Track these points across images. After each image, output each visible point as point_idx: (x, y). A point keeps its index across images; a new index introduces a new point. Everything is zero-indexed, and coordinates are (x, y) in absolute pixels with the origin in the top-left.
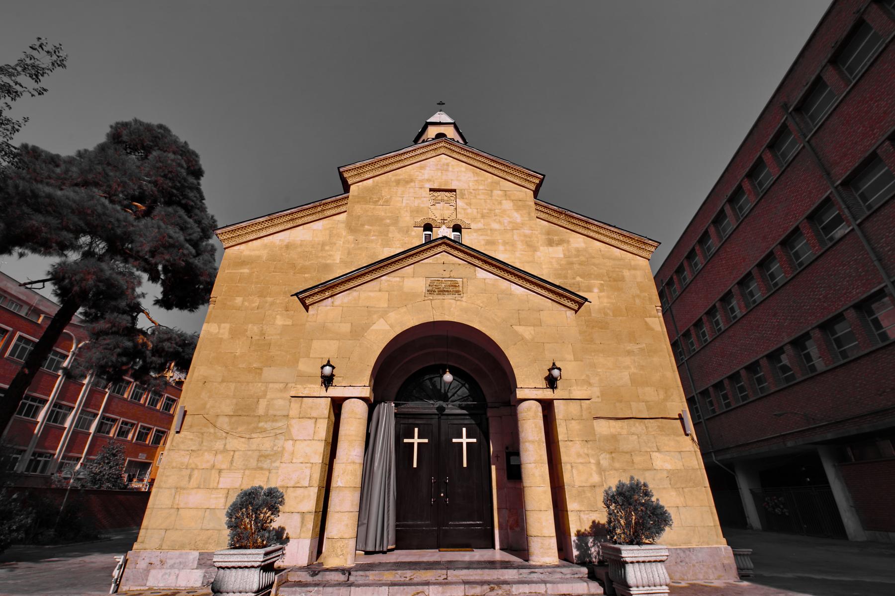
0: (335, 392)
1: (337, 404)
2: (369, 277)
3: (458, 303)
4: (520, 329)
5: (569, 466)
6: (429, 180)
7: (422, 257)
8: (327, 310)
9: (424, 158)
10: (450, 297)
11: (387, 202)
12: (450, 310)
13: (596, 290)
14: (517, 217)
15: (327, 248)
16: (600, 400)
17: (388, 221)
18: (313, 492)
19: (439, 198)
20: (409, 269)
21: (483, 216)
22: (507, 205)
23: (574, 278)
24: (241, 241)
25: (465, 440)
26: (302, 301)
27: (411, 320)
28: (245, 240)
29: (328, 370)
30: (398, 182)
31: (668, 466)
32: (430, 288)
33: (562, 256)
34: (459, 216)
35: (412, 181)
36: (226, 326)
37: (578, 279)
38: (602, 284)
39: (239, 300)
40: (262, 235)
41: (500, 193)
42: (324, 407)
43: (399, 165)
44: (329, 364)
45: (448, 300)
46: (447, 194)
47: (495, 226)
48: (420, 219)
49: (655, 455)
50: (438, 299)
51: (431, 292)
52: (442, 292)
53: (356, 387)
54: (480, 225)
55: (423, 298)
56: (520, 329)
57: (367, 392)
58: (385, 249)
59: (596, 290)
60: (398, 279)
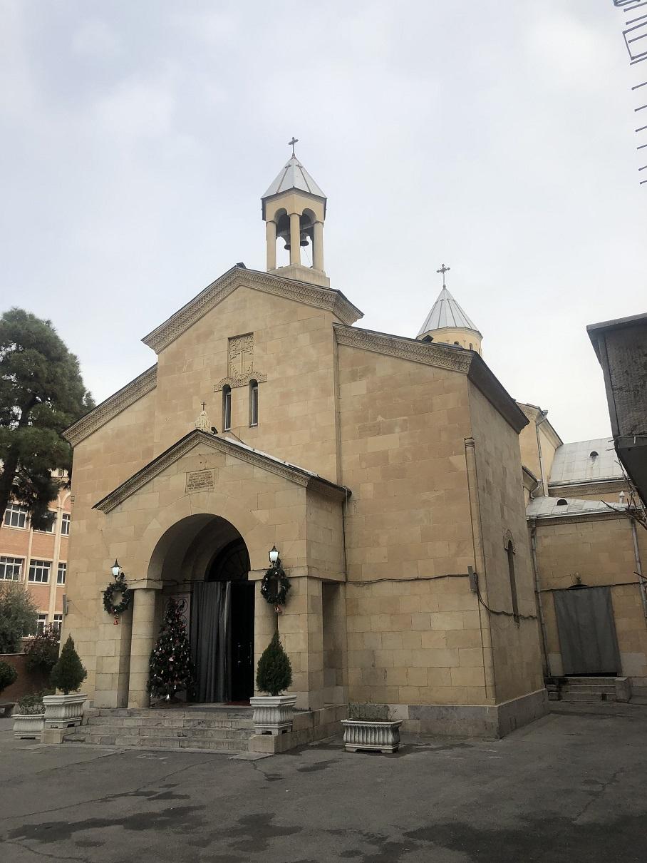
2: (145, 481)
7: (182, 453)
11: (190, 366)
12: (206, 504)
13: (397, 430)
15: (148, 430)
16: (386, 560)
20: (174, 467)
21: (279, 363)
22: (305, 339)
23: (375, 419)
24: (83, 437)
27: (177, 518)
28: (86, 435)
31: (448, 628)
33: (365, 392)
34: (255, 368)
35: (211, 333)
36: (84, 522)
37: (380, 418)
38: (405, 420)
41: (296, 324)
43: (198, 316)
46: (245, 339)
47: (291, 372)
48: (219, 381)
49: (434, 616)
52: (199, 485)
55: (184, 494)
59: (397, 430)
60: (166, 478)
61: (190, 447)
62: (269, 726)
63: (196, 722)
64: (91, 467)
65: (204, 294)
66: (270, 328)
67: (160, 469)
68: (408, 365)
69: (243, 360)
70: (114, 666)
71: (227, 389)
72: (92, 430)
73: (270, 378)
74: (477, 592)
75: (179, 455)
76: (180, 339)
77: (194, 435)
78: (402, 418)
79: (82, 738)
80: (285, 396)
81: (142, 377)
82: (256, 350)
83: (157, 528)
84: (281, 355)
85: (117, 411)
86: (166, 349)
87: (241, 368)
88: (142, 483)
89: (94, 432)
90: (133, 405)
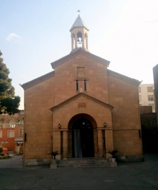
0: (61, 130)
1: (62, 132)
4: (98, 114)
12: (83, 111)
26: (51, 110)
27: (76, 114)
29: (59, 126)
42: (60, 132)
50: (80, 108)
51: (79, 106)
52: (82, 106)
57: (67, 130)
86: (57, 67)
87: (81, 75)
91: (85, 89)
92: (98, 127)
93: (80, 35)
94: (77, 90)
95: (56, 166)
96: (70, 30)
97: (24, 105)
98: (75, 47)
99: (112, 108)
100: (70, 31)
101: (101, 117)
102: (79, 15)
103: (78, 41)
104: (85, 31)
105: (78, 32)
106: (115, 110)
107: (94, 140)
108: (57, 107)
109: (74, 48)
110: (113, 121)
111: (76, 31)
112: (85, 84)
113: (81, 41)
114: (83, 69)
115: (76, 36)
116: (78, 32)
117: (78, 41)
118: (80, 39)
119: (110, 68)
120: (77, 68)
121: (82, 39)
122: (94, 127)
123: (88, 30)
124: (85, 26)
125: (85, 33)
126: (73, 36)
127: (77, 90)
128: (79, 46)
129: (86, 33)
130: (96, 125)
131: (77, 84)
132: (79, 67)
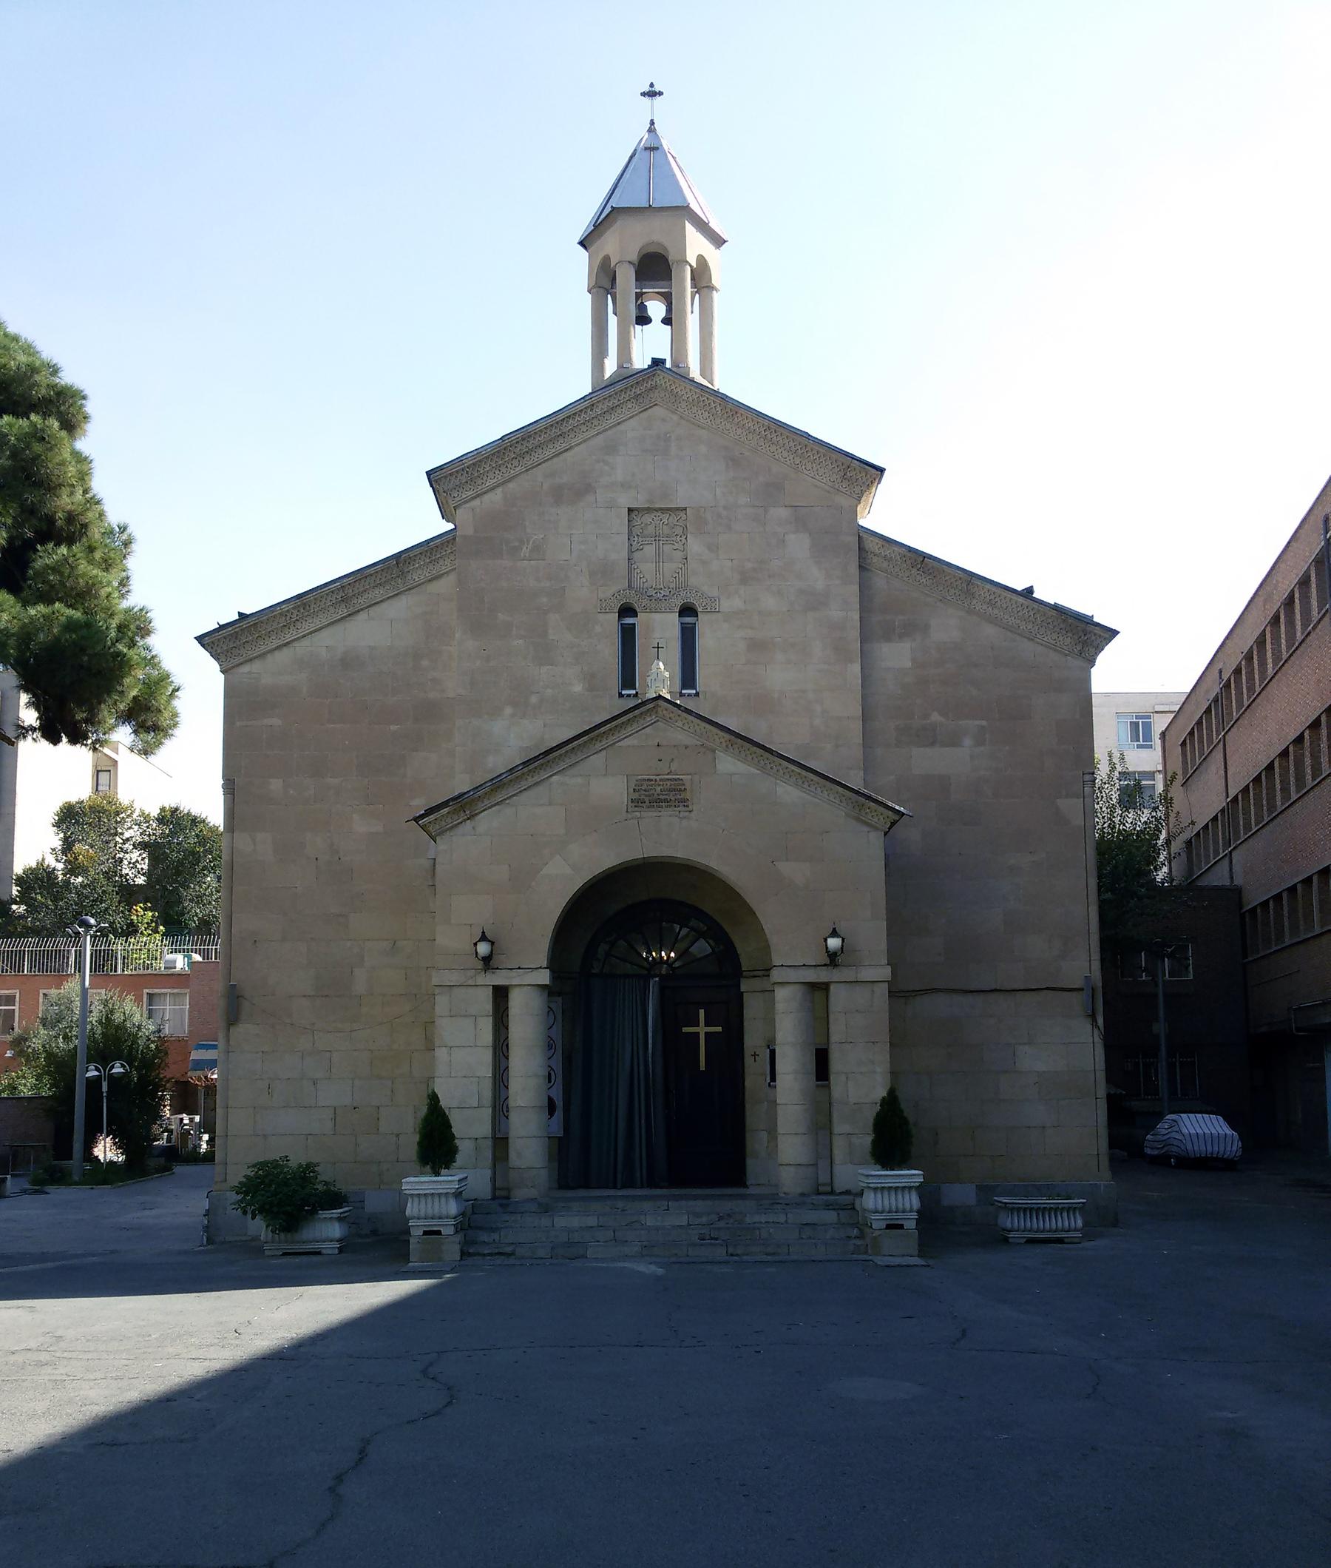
0: (500, 979)
1: (501, 994)
2: (531, 781)
3: (685, 822)
4: (786, 868)
5: (843, 1078)
6: (625, 486)
7: (617, 736)
8: (466, 845)
9: (612, 421)
10: (670, 811)
11: (538, 549)
13: (968, 742)
14: (817, 578)
15: (425, 663)
17: (545, 600)
18: (487, 1113)
19: (651, 529)
20: (597, 760)
21: (745, 580)
22: (799, 545)
24: (252, 654)
25: (702, 1030)
27: (608, 859)
29: (483, 949)
30: (559, 495)
32: (636, 796)
33: (909, 664)
37: (935, 717)
38: (983, 727)
39: (276, 785)
40: (289, 638)
41: (782, 513)
42: (484, 1001)
43: (558, 447)
44: (484, 938)
45: (667, 817)
47: (770, 602)
48: (614, 590)
51: (637, 803)
52: (657, 802)
53: (529, 979)
54: (737, 603)
56: (786, 868)
57: (544, 977)
58: (544, 669)
59: (968, 742)
60: (580, 780)
61: (635, 727)
62: (900, 1216)
63: (714, 1217)
64: (276, 722)
65: (581, 407)
66: (725, 508)
67: (568, 761)
68: (990, 631)
69: (660, 558)
70: (482, 1127)
71: (627, 611)
72: (277, 643)
73: (726, 605)
74: (1093, 1016)
75: (611, 739)
76: (511, 485)
77: (651, 706)
78: (977, 722)
79: (508, 1249)
80: (756, 646)
81: (416, 552)
82: (695, 546)
83: (563, 876)
84: (749, 565)
85: (343, 611)
86: (476, 503)
88: (524, 784)
89: (279, 648)
90: (384, 605)
91: (688, 677)
92: (777, 961)
93: (655, 268)
94: (628, 678)
95: (457, 1247)
96: (579, 235)
97: (224, 786)
98: (620, 366)
99: (893, 824)
100: (582, 243)
101: (809, 895)
102: (652, 123)
103: (643, 319)
104: (696, 245)
105: (642, 255)
106: (911, 835)
107: (748, 1060)
108: (463, 806)
109: (610, 367)
110: (901, 923)
111: (624, 246)
112: (688, 636)
113: (667, 321)
114: (673, 520)
115: (626, 278)
116: (642, 255)
117: (643, 319)
118: (656, 309)
119: (884, 514)
120: (630, 510)
121: (669, 310)
122: (745, 964)
123: (718, 241)
124: (694, 206)
125: (692, 259)
126: (603, 282)
127: (628, 678)
128: (650, 344)
129: (701, 259)
130: (766, 949)
131: (628, 635)
132: (641, 496)
